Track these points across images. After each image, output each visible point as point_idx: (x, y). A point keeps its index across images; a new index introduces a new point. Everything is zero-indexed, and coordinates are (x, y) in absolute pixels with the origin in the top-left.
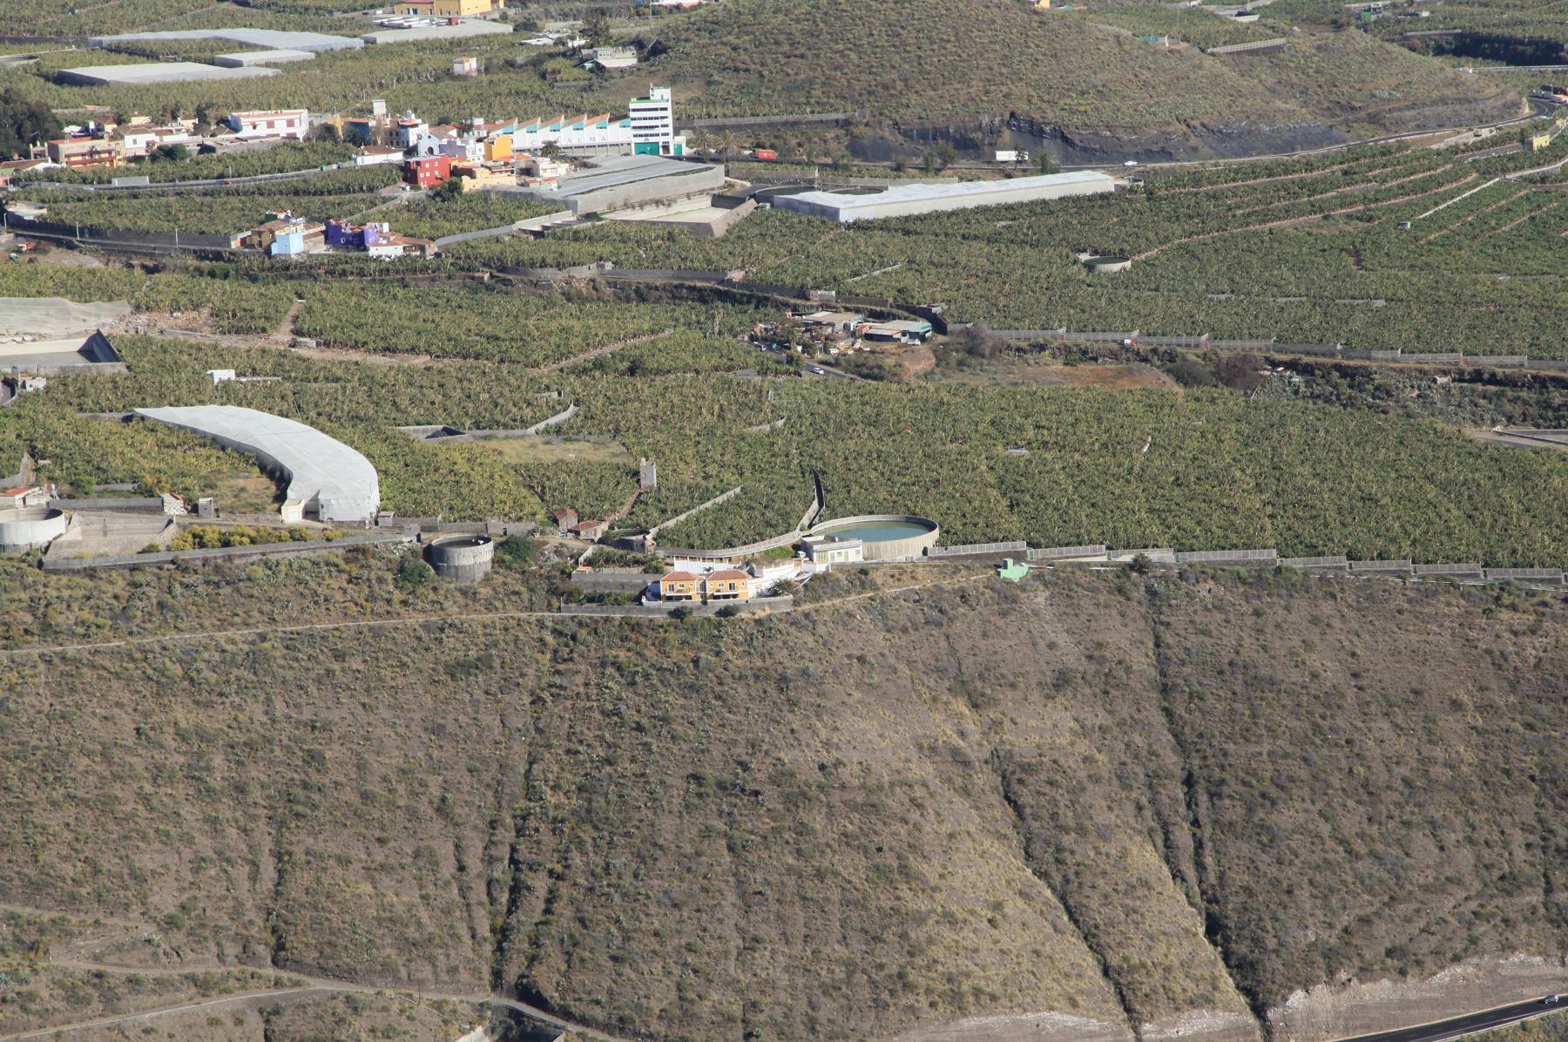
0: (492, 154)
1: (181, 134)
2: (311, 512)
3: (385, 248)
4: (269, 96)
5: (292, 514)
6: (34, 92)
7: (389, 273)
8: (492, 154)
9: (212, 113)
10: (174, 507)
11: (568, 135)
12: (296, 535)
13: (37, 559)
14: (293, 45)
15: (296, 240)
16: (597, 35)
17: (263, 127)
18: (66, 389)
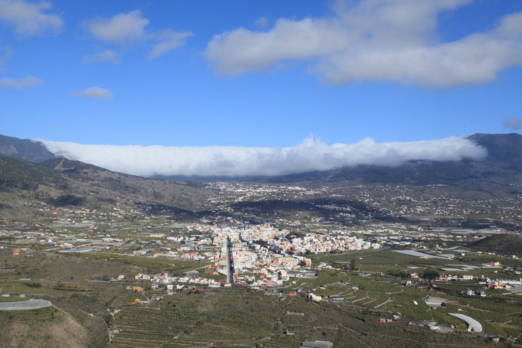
0: (499, 284)
1: (455, 278)
2: (472, 330)
3: (483, 295)
4: (468, 273)
5: (469, 330)
6: (436, 271)
7: (483, 298)
8: (499, 284)
9: (460, 275)
10: (453, 327)
11: (510, 282)
12: (470, 333)
13: (434, 331)
14: (471, 267)
15: (470, 293)
16: (515, 269)
17: (466, 278)
18: (439, 309)
